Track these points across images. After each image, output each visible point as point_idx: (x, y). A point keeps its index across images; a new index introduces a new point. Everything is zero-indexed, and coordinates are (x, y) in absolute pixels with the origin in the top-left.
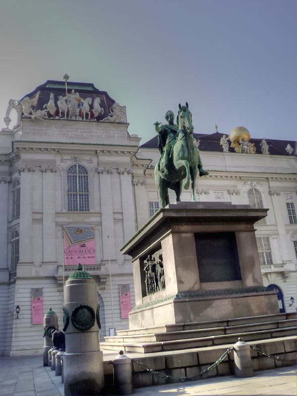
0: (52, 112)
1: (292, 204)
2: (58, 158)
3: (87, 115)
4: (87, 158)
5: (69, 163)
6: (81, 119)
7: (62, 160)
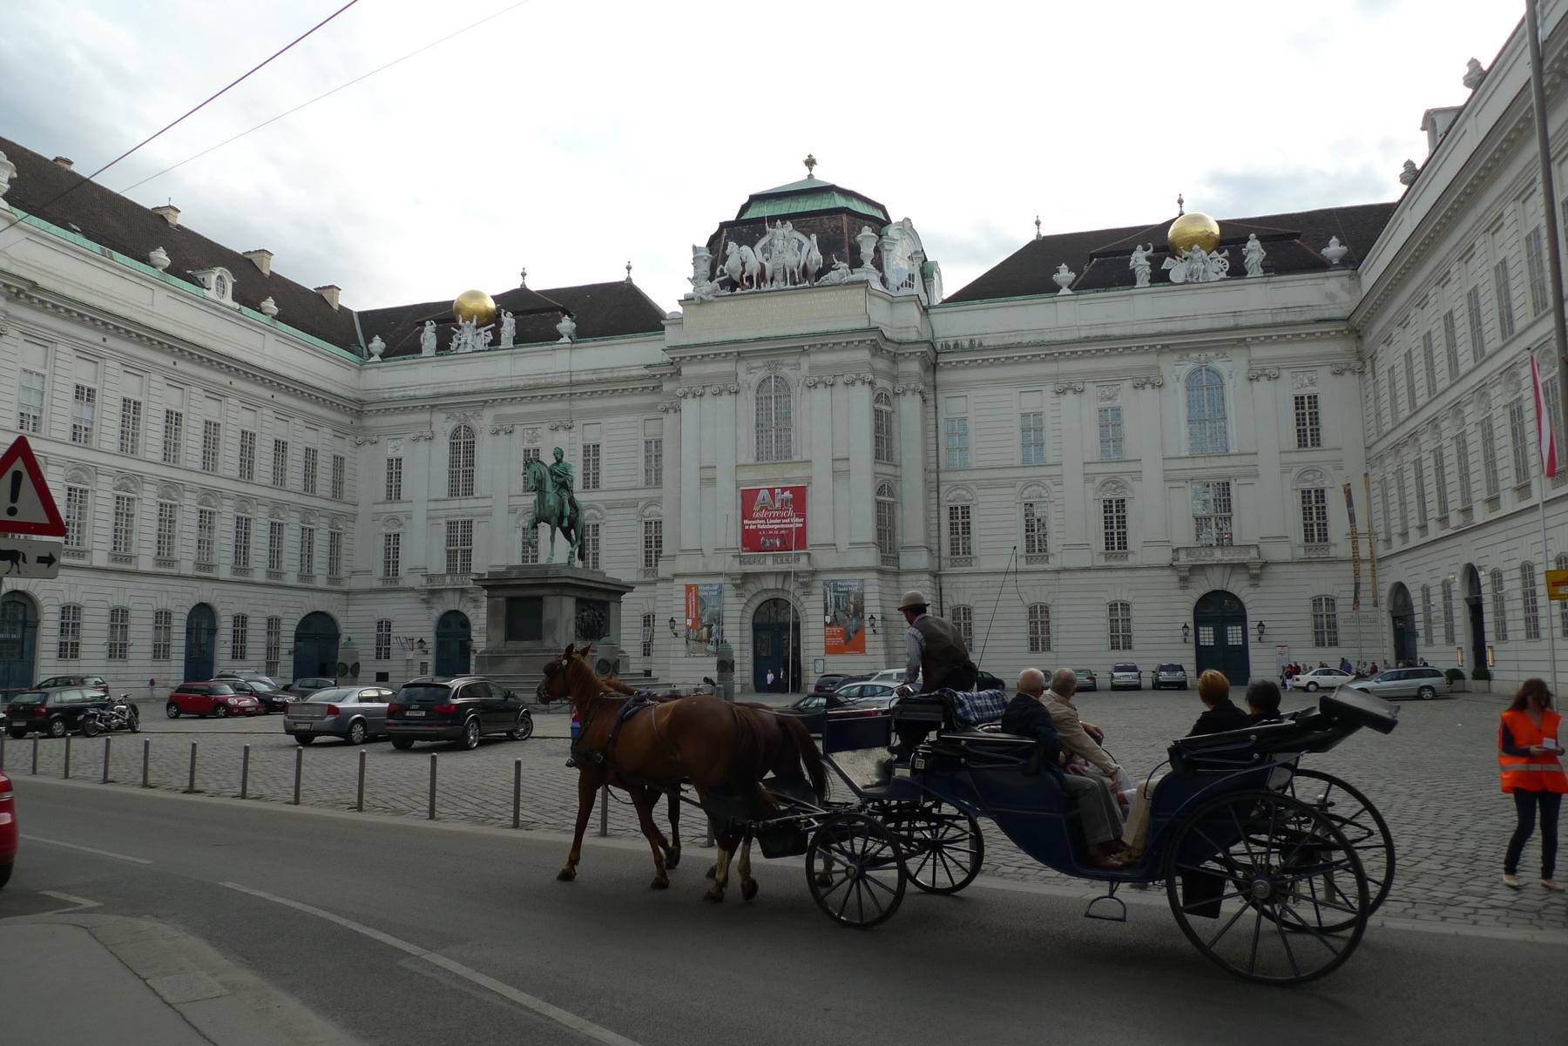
0: (736, 277)
1: (1313, 399)
2: (742, 367)
3: (792, 273)
4: (790, 360)
5: (760, 375)
6: (782, 285)
7: (749, 370)
